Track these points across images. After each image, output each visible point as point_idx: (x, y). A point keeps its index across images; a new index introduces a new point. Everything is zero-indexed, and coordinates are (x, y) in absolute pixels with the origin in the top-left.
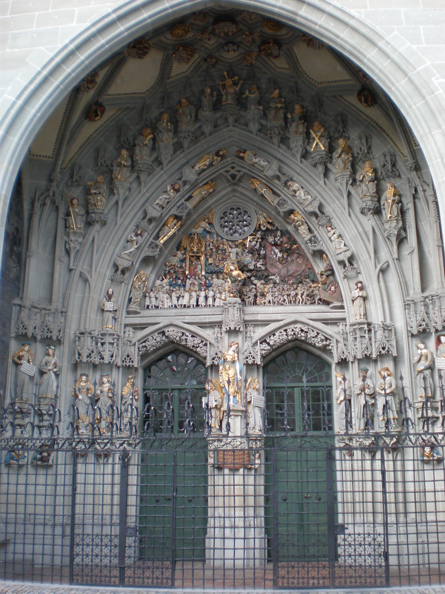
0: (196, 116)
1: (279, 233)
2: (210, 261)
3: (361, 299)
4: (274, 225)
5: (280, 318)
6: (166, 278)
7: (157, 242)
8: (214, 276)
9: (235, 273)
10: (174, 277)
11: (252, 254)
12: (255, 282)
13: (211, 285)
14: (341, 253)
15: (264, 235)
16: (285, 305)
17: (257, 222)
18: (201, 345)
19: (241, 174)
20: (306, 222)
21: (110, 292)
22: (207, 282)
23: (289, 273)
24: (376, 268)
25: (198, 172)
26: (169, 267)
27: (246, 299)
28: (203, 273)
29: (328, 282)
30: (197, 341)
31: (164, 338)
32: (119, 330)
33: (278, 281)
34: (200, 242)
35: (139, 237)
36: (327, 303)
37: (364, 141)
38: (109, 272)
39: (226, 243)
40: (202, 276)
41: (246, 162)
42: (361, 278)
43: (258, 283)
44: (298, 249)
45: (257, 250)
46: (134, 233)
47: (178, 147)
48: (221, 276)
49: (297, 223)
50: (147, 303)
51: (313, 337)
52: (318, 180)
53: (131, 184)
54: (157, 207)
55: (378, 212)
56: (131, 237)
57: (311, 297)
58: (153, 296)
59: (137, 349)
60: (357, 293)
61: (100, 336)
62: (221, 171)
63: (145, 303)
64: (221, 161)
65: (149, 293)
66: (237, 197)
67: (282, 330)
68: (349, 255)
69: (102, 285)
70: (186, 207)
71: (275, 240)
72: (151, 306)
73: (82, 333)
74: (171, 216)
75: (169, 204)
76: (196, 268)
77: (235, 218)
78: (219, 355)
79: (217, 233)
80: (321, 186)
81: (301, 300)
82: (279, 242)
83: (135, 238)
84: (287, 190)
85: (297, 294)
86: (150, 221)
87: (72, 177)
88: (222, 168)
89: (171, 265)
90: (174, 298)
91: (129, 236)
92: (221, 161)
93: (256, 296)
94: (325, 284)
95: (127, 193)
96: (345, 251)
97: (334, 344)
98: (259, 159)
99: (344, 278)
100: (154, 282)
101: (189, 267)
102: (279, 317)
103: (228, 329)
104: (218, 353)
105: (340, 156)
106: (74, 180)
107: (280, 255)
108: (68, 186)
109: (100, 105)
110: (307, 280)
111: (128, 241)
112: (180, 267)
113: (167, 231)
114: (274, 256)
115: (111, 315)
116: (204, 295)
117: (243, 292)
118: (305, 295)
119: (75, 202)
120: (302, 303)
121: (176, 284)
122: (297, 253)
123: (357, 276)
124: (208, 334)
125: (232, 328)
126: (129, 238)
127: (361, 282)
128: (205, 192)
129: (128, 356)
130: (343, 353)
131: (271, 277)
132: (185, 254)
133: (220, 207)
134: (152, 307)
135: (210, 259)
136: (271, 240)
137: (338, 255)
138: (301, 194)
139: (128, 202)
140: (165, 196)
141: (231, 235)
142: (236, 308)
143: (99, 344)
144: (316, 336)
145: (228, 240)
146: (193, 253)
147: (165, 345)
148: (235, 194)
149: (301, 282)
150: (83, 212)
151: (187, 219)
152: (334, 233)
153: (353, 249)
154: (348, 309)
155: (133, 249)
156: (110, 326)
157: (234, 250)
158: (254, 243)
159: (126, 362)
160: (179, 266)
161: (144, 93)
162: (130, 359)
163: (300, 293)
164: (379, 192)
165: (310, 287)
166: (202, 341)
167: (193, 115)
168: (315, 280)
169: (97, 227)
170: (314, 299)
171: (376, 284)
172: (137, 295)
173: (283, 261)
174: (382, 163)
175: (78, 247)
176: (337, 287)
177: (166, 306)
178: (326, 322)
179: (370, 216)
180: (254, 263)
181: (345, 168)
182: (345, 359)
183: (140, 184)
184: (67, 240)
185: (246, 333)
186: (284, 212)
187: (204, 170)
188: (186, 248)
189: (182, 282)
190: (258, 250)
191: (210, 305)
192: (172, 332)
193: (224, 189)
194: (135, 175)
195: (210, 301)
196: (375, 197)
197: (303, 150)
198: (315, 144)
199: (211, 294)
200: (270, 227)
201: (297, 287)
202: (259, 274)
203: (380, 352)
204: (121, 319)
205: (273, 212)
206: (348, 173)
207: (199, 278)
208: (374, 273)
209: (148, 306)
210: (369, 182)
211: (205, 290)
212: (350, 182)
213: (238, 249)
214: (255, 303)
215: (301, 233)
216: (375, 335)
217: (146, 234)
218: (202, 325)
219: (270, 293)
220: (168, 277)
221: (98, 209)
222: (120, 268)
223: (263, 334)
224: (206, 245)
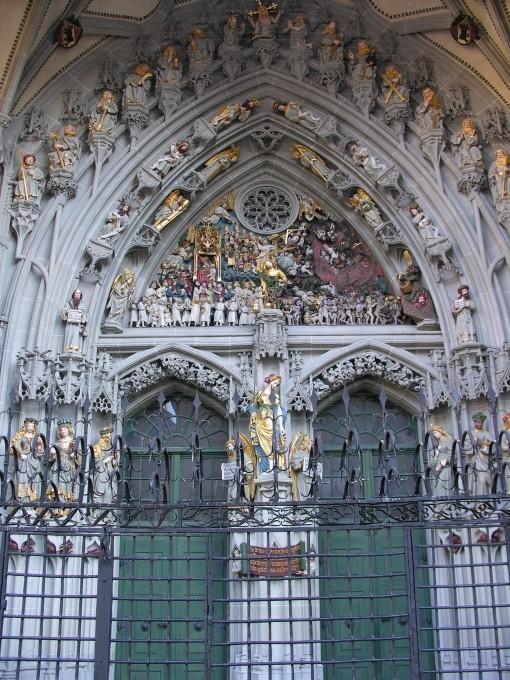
0: (216, 52)
1: (333, 226)
2: (231, 261)
3: (469, 311)
4: (324, 215)
5: (343, 342)
7: (152, 227)
9: (273, 272)
13: (233, 295)
14: (435, 245)
17: (300, 210)
18: (219, 382)
19: (279, 137)
20: (377, 206)
21: (78, 296)
24: (488, 266)
28: (219, 280)
30: (213, 375)
31: (160, 370)
32: (91, 356)
33: (333, 292)
34: (214, 236)
36: (412, 321)
37: (459, 94)
38: (76, 267)
39: (253, 237)
41: (288, 119)
42: (464, 281)
43: (305, 295)
44: (362, 248)
47: (189, 90)
48: (247, 284)
50: (134, 318)
51: (394, 371)
53: (116, 140)
54: (155, 174)
55: (485, 188)
59: (116, 386)
60: (461, 303)
61: (59, 361)
62: (250, 132)
64: (251, 115)
65: (137, 305)
66: (270, 174)
67: (346, 360)
68: (447, 248)
69: (65, 284)
70: (198, 179)
71: (327, 235)
72: (138, 324)
73: (30, 356)
75: (173, 171)
78: (250, 397)
80: (400, 152)
81: (372, 318)
83: (119, 216)
84: (349, 159)
85: (365, 310)
86: (145, 192)
87: (27, 127)
88: (249, 128)
89: (171, 267)
90: (176, 313)
91: (111, 214)
92: (251, 115)
93: (303, 312)
94: (410, 293)
95: (110, 152)
96: (440, 242)
97: (426, 380)
98: (309, 112)
99: (439, 282)
100: (144, 290)
102: (342, 340)
103: (264, 356)
104: (248, 393)
105: (426, 111)
106: (31, 130)
107: (334, 255)
108: (20, 140)
109: (77, 23)
110: (377, 292)
111: (108, 222)
114: (327, 258)
115: (78, 329)
116: (223, 308)
118: (377, 310)
119: (29, 160)
120: (374, 322)
121: (179, 295)
122: (361, 254)
123: (459, 280)
124: (228, 364)
125: (271, 354)
126: (110, 217)
127: (467, 288)
129: (102, 396)
130: (442, 394)
132: (192, 251)
133: (243, 188)
134: (141, 325)
137: (430, 247)
138: (371, 162)
139: (109, 166)
140: (167, 158)
143: (57, 375)
144: (400, 369)
145: (256, 234)
146: (205, 250)
147: (161, 381)
148: (268, 170)
149: (367, 295)
150: (42, 176)
151: (198, 199)
152: (423, 217)
153: (451, 239)
154: (446, 330)
156: (75, 347)
157: (267, 247)
158: (295, 238)
159: (99, 405)
160: (182, 268)
161: (141, 19)
162: (106, 401)
163: (370, 307)
164: (485, 164)
166: (221, 377)
167: (212, 48)
169: (61, 197)
171: (491, 289)
172: (119, 304)
174: (487, 124)
175: (30, 227)
176: (428, 296)
177: (163, 324)
178: (412, 348)
179: (474, 193)
180: (296, 266)
181: (435, 126)
182: (446, 402)
183: (129, 141)
184: (14, 215)
185: (291, 364)
186: (343, 191)
187: (224, 127)
190: (303, 250)
192: (172, 361)
193: (250, 159)
194: (122, 128)
195: (232, 317)
196: (480, 166)
197: (372, 103)
198: (389, 94)
199: (233, 306)
200: (319, 216)
202: (305, 282)
203: (505, 389)
204: (94, 340)
205: (325, 195)
206: (440, 132)
208: (487, 274)
210: (471, 146)
212: (444, 146)
214: (302, 322)
216: (495, 363)
217: (136, 213)
218: (221, 351)
220: (166, 283)
221: (64, 171)
222: (95, 259)
223: (318, 365)
224: (223, 240)
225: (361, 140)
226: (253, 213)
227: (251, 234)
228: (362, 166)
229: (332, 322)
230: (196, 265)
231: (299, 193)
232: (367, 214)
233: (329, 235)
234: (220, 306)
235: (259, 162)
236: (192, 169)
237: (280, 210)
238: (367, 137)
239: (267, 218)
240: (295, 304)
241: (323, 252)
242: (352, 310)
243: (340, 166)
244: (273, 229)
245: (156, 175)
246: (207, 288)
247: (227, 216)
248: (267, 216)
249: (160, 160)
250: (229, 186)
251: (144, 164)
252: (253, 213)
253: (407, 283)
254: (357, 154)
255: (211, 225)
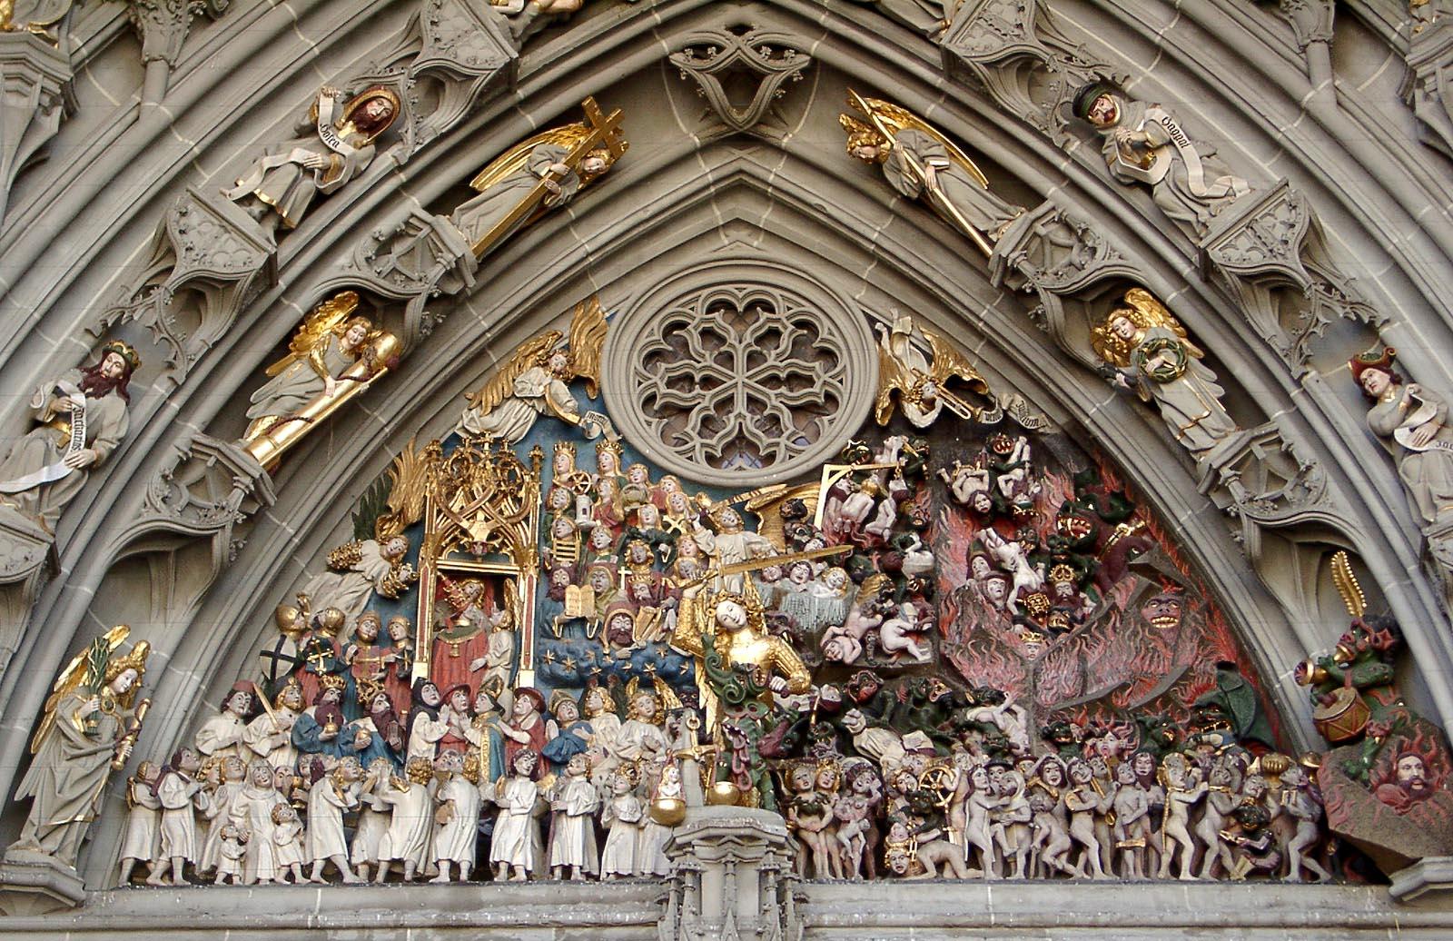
2: (577, 602)
4: (988, 403)
6: (273, 702)
8: (599, 697)
9: (749, 650)
10: (331, 697)
11: (847, 565)
12: (874, 739)
15: (926, 457)
16: (1082, 881)
19: (793, 65)
20: (1211, 360)
22: (552, 730)
23: (1094, 691)
25: (519, 24)
26: (302, 632)
27: (811, 838)
28: (527, 679)
29: (1375, 726)
34: (510, 486)
35: (113, 403)
40: (519, 693)
44: (1146, 547)
45: (881, 546)
46: (79, 376)
48: (644, 702)
49: (1152, 365)
50: (139, 845)
52: (1289, 78)
54: (243, 218)
56: (58, 392)
57: (1253, 834)
58: (183, 800)
62: (664, 45)
63: (123, 846)
70: (434, 245)
71: (995, 487)
72: (158, 869)
74: (330, 295)
76: (483, 647)
77: (740, 359)
79: (624, 441)
81: (1189, 847)
82: (1022, 499)
83: (79, 399)
89: (317, 625)
93: (880, 823)
95: (51, 124)
101: (434, 645)
107: (1026, 576)
110: (1216, 738)
111: (35, 424)
112: (373, 641)
113: (301, 390)
114: (995, 586)
117: (795, 792)
118: (1212, 814)
120: (1196, 870)
122: (1145, 570)
126: (42, 401)
128: (559, 167)
131: (972, 714)
132: (410, 556)
134: (169, 872)
135: (572, 592)
136: (973, 485)
141: (711, 459)
142: (751, 874)
145: (690, 485)
146: (466, 552)
152: (1415, 404)
155: (61, 469)
157: (733, 543)
160: (367, 630)
163: (1178, 801)
165: (1242, 768)
168: (1266, 736)
170: (1272, 840)
173: (1047, 614)
186: (1065, 298)
188: (420, 524)
189: (383, 731)
191: (567, 870)
195: (571, 842)
199: (577, 797)
201: (1157, 761)
207: (498, 708)
209: (141, 868)
211: (534, 776)
213: (751, 536)
214: (876, 866)
215: (1181, 422)
219: (979, 796)
220: (290, 694)
224: (547, 507)
225: (1142, 74)
226: (680, 396)
227: (669, 484)
228: (1148, 188)
229: (1007, 865)
230: (427, 614)
231: (880, 307)
232: (1167, 392)
233: (1007, 490)
234: (521, 795)
235: (705, 171)
236: (413, 204)
237: (795, 379)
238: (1170, 61)
239: (740, 417)
240: (846, 786)
241: (981, 565)
242: (1096, 815)
243: (1050, 188)
244: (770, 458)
245: (250, 226)
246: (472, 714)
247: (566, 404)
248: (740, 406)
249: (267, 162)
250: (581, 277)
251: (205, 179)
252: (680, 396)
253: (1346, 695)
254: (1121, 133)
255: (497, 442)
